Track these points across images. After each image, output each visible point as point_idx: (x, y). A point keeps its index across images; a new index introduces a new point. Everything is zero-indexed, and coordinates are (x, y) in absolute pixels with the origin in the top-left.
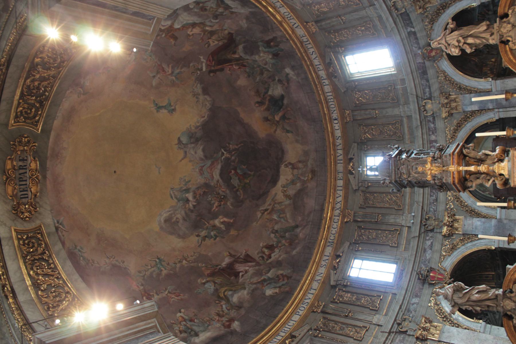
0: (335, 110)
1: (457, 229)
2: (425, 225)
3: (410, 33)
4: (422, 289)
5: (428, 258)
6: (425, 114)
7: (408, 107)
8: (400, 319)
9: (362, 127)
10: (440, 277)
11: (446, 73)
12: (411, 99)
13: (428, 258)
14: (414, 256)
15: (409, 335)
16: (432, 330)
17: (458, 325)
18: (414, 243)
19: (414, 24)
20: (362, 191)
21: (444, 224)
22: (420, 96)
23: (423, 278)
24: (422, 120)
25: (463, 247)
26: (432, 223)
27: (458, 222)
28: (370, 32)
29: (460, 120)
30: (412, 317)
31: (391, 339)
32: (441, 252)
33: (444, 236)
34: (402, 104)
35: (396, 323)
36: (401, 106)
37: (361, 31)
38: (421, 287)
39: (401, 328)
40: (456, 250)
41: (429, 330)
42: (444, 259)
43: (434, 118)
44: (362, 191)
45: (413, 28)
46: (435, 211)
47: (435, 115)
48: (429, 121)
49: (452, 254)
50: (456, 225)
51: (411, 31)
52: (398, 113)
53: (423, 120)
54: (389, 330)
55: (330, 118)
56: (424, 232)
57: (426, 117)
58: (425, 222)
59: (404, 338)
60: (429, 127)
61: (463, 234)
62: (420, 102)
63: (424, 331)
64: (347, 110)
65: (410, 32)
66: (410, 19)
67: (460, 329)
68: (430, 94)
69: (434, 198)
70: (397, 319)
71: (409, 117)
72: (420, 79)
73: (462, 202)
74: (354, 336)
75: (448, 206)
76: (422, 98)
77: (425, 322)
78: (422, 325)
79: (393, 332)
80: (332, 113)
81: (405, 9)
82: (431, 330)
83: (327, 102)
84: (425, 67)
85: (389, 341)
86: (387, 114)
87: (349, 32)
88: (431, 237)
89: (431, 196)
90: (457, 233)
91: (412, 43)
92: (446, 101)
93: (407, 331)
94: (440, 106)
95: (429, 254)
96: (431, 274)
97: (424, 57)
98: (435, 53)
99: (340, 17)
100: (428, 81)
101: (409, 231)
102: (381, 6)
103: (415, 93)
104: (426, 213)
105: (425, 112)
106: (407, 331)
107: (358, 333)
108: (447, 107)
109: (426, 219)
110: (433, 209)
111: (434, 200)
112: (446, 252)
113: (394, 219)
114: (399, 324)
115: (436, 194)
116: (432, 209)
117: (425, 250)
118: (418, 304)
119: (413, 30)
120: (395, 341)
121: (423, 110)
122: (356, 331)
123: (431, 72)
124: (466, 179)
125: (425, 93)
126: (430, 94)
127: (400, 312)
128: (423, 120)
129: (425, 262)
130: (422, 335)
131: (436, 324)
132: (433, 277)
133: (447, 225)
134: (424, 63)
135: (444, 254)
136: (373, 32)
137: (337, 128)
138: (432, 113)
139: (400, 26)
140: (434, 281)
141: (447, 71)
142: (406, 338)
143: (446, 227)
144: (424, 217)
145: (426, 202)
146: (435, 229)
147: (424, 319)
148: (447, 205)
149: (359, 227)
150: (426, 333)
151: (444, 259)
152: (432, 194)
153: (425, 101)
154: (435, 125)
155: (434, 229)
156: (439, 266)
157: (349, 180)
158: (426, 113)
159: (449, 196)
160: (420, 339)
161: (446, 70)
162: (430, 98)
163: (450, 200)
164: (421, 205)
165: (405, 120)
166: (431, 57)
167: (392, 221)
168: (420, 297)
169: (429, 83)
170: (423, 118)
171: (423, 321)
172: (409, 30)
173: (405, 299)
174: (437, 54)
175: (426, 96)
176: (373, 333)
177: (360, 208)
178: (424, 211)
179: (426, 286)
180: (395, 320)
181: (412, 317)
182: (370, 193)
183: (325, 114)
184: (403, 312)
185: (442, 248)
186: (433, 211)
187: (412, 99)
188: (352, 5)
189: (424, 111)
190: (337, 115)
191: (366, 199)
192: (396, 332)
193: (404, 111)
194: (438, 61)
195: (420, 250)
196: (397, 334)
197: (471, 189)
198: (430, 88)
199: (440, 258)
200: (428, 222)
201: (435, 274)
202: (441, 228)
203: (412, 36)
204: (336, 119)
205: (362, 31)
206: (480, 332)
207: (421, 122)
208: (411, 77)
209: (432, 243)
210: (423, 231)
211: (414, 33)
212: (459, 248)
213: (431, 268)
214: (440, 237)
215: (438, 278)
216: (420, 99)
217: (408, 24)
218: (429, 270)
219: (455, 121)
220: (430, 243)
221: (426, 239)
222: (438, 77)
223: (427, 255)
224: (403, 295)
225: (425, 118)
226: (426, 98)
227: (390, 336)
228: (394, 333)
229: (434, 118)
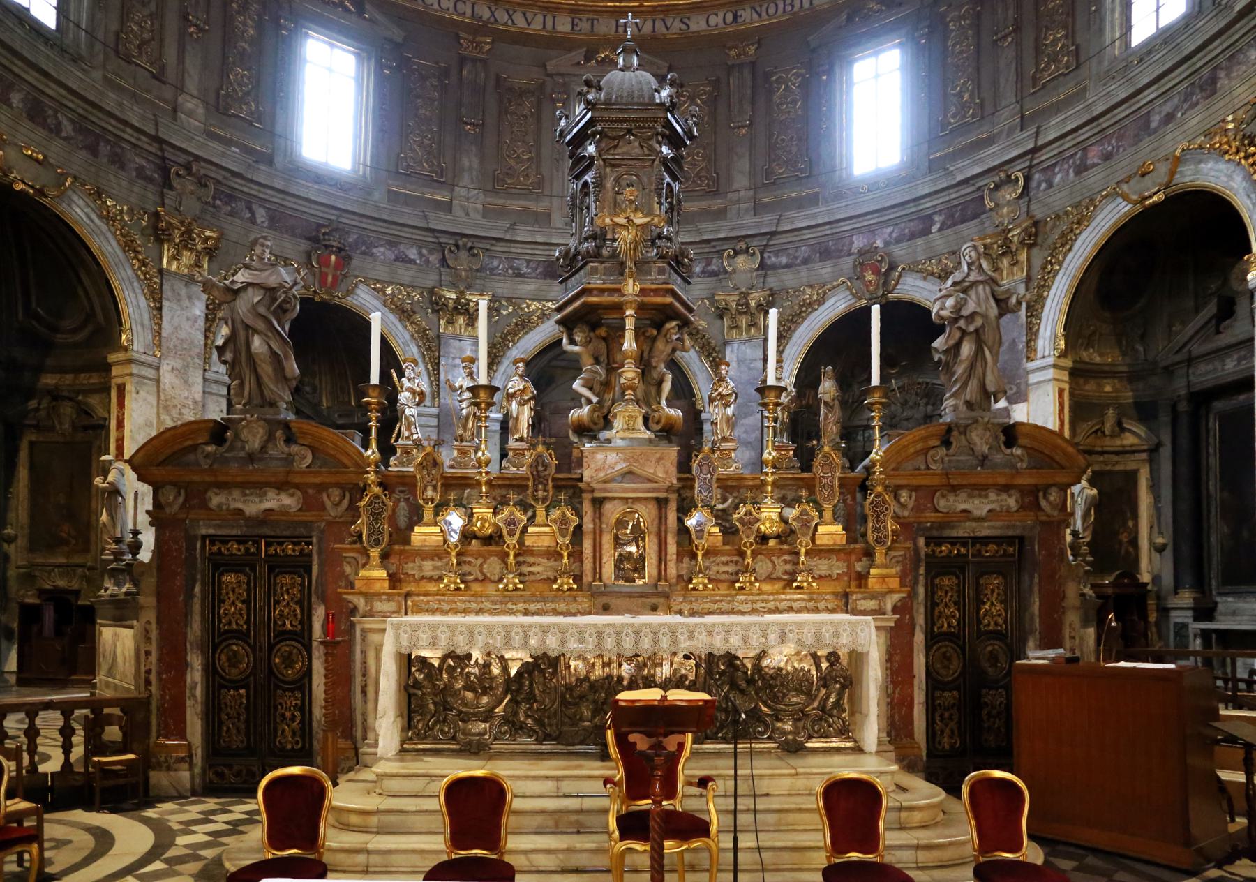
1: (450, 322)
2: (457, 246)
3: (928, 220)
4: (294, 235)
5: (374, 250)
6: (726, 253)
7: (747, 210)
8: (202, 172)
10: (330, 278)
11: (819, 305)
12: (767, 218)
13: (374, 250)
14: (376, 215)
15: (162, 195)
16: (187, 257)
17: (213, 320)
18: (409, 216)
19: (948, 232)
20: (542, 85)
21: (462, 292)
22: (771, 243)
23: (322, 237)
24: (713, 244)
25: (407, 336)
26: (462, 262)
27: (468, 325)
28: (954, 116)
29: (704, 336)
30: (214, 206)
31: (140, 143)
32: (392, 283)
33: (432, 292)
35: (191, 159)
37: (960, 91)
38: (298, 231)
39: (178, 174)
40: (400, 321)
41: (186, 247)
42: (374, 289)
43: (714, 274)
44: (542, 85)
45: (940, 230)
46: (492, 270)
48: (709, 263)
49: (390, 309)
50: (461, 321)
51: (932, 223)
53: (714, 247)
54: (165, 137)
56: (440, 243)
57: (720, 253)
58: (465, 245)
59: (150, 180)
61: (438, 336)
63: (182, 235)
65: (932, 220)
66: (963, 221)
67: (201, 323)
68: (774, 267)
69: (524, 270)
70: (203, 164)
71: (721, 214)
72: (811, 242)
73: (516, 335)
74: (126, 34)
75: (504, 303)
76: (766, 246)
77: (208, 238)
78: (196, 231)
79: (162, 150)
81: (991, 210)
82: (186, 254)
84: (840, 257)
85: (132, 136)
87: (967, 58)
88: (428, 261)
89: (528, 262)
90: (442, 322)
91: (903, 225)
92: (753, 303)
93: (171, 188)
94: (743, 290)
95: (383, 254)
96: (333, 258)
97: (868, 252)
98: (870, 281)
99: (1014, 30)
100: (806, 261)
101: (438, 205)
102: (1016, 144)
104: (487, 250)
105: (732, 253)
106: (171, 188)
107: (139, 47)
108: (737, 305)
109: (471, 248)
110: (497, 267)
111: (518, 269)
112: (393, 295)
113: (471, 168)
114: (188, 167)
115: (534, 274)
116: (495, 263)
117: (392, 244)
118: (253, 220)
119: (934, 229)
120: (136, 155)
121: (737, 248)
122: (144, 43)
123: (825, 270)
124: (594, 326)
125: (777, 253)
126: (774, 267)
127: (223, 173)
128: (714, 247)
129: (364, 243)
130: (168, 229)
131: (206, 266)
132: (327, 264)
133: (458, 299)
134: (850, 255)
135: (389, 291)
136: (950, 124)
139: (953, 196)
140: (318, 263)
141: (822, 308)
142: (151, 186)
143: (453, 296)
144: (476, 245)
145: (513, 250)
146: (448, 270)
147: (214, 235)
148: (509, 299)
149: (446, 73)
150: (177, 241)
151: (374, 289)
152: (533, 265)
153: (758, 253)
155: (448, 266)
156: (357, 277)
157: (571, 50)
158: (729, 256)
159: (528, 306)
160: (158, 222)
161: (828, 304)
162: (762, 266)
163: (519, 308)
164: (508, 237)
166: (862, 271)
167: (466, 162)
168: (271, 227)
169: (799, 265)
170: (718, 248)
171: (208, 234)
172: (936, 218)
173: (262, 189)
174: (867, 286)
175: (769, 257)
176: (148, 91)
177: (497, 75)
178: (492, 245)
179: (304, 245)
180: (197, 158)
181: (214, 206)
182: (539, 102)
184: (225, 181)
185: (402, 285)
186: (490, 266)
188: (1037, 64)
189: (734, 250)
191: (522, 93)
192: (164, 159)
193: (738, 202)
194: (848, 288)
195: (391, 232)
196: (158, 161)
197: (565, 341)
198: (788, 266)
199: (378, 281)
200: (463, 255)
201: (338, 266)
202: (454, 286)
203: (921, 227)
205: (960, 95)
206: (205, 370)
207: (708, 241)
208: (820, 221)
209: (412, 261)
210: (441, 240)
211: (926, 232)
212: (406, 327)
213: (350, 258)
214: (430, 281)
215: (326, 275)
216: (765, 243)
217: (952, 216)
218: (343, 253)
219: (703, 323)
220: (412, 257)
221: (420, 247)
222: (811, 286)
223: (382, 249)
224: (268, 183)
225: (718, 251)
226: (766, 255)
227: (149, 141)
228: (159, 153)
229: (714, 274)
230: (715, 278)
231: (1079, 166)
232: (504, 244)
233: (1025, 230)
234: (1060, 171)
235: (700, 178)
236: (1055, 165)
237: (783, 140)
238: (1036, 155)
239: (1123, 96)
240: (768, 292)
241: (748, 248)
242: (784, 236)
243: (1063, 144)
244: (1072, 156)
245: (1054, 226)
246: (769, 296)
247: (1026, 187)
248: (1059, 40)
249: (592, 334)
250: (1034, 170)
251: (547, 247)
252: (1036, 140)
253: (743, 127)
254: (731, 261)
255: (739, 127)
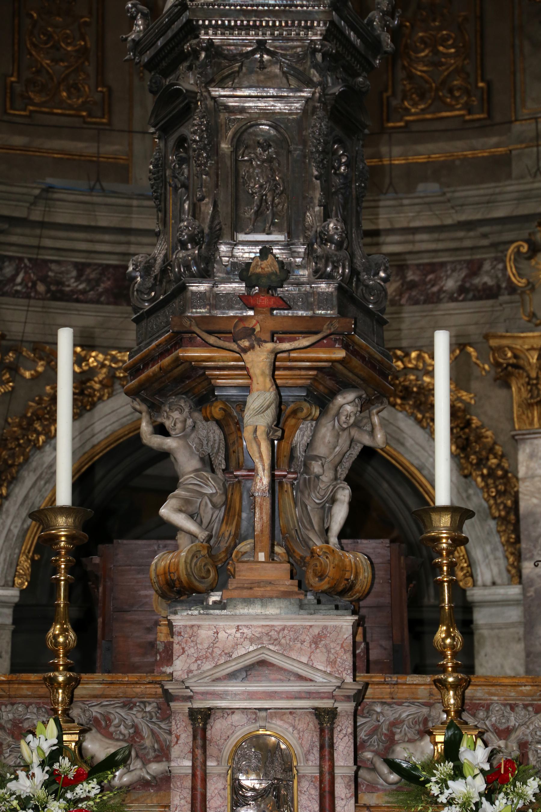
6: (512, 248)
47: (502, 299)
53: (485, 236)
60: (443, 265)
89: (81, 268)
105: (525, 249)
111: (60, 283)
138: (520, 282)
154: (452, 299)
158: (518, 253)
164: (36, 216)
170: (495, 239)
225: (494, 245)
230: (490, 302)
232: (27, 231)
251: (122, 238)
254: (524, 264)
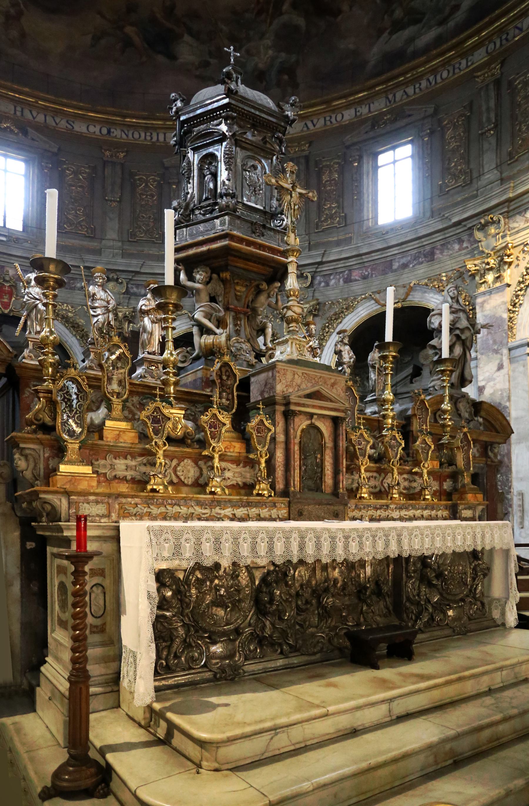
0: (127, 136)
9: (87, 171)
12: (134, 262)
22: (134, 278)
34: (124, 247)
36: (120, 244)
52: (108, 237)
55: (114, 123)
62: (124, 276)
64: (124, 156)
76: (130, 279)
80: (123, 131)
83: (146, 128)
86: (108, 219)
92: (120, 314)
103: (142, 271)
121: (111, 276)
125: (138, 286)
137: (92, 129)
162: (127, 292)
165: (94, 244)
175: (132, 288)
183: (125, 116)
187: (134, 264)
188: (319, 218)
190: (119, 136)
204: (109, 132)
216: (130, 277)
226: (130, 286)
231: (347, 278)
233: (313, 306)
234: (334, 278)
235: (81, 226)
236: (331, 274)
237: (143, 217)
238: (320, 266)
239: (380, 247)
240: (132, 310)
241: (118, 279)
242: (144, 276)
243: (337, 264)
244: (342, 272)
245: (330, 307)
246: (133, 312)
247: (312, 283)
248: (334, 208)
249: (215, 276)
250: (316, 274)
252: (322, 258)
253: (114, 201)
255: (111, 201)
